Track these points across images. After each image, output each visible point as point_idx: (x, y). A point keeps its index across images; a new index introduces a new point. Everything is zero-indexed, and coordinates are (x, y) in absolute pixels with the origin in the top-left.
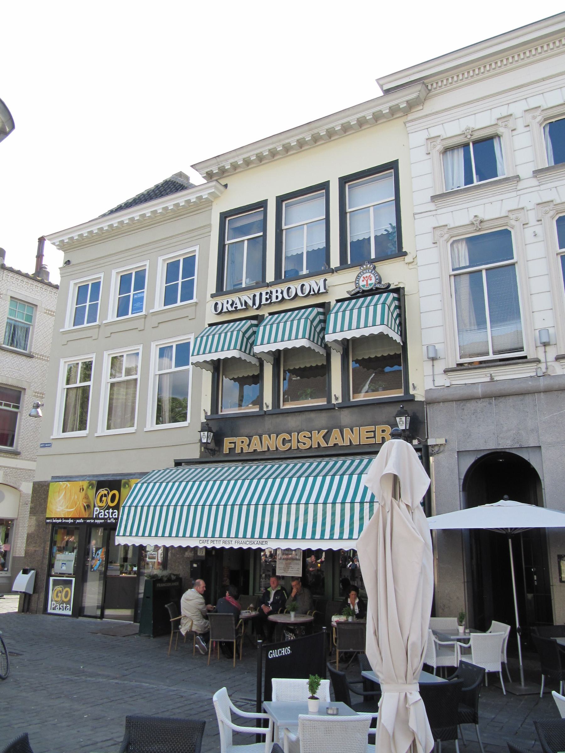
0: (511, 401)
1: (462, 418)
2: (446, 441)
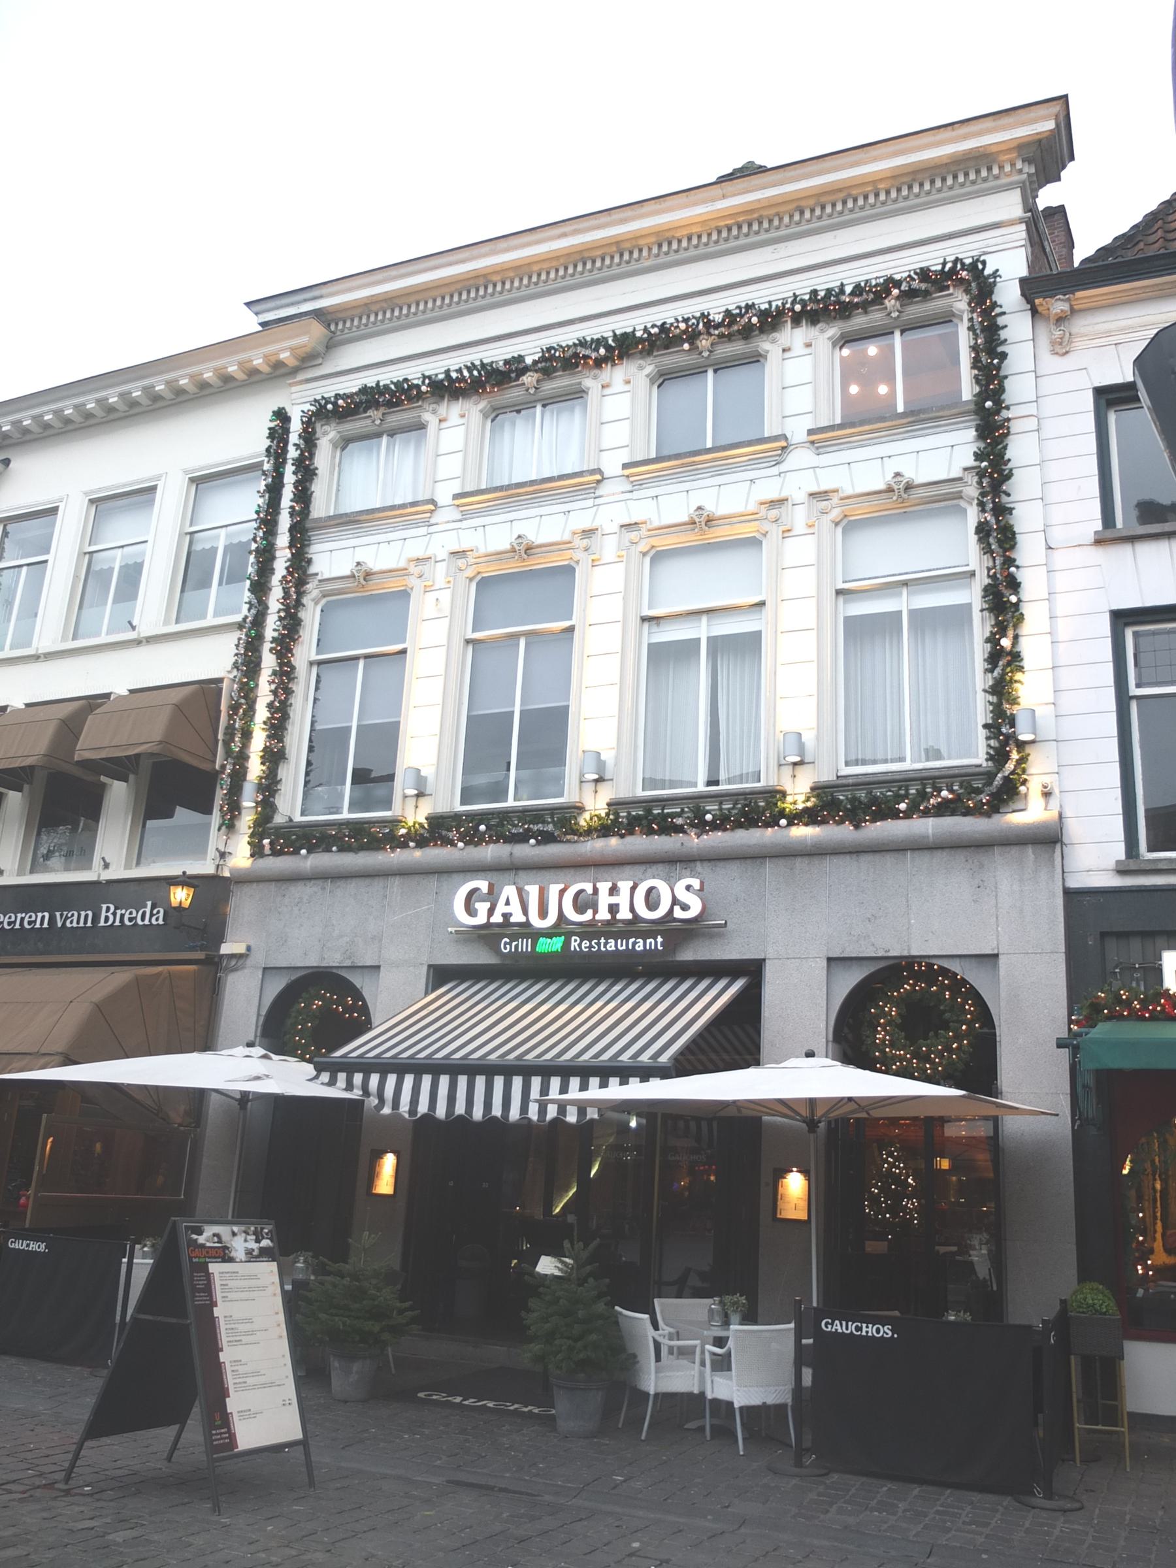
0: (352, 886)
1: (280, 910)
2: (249, 948)
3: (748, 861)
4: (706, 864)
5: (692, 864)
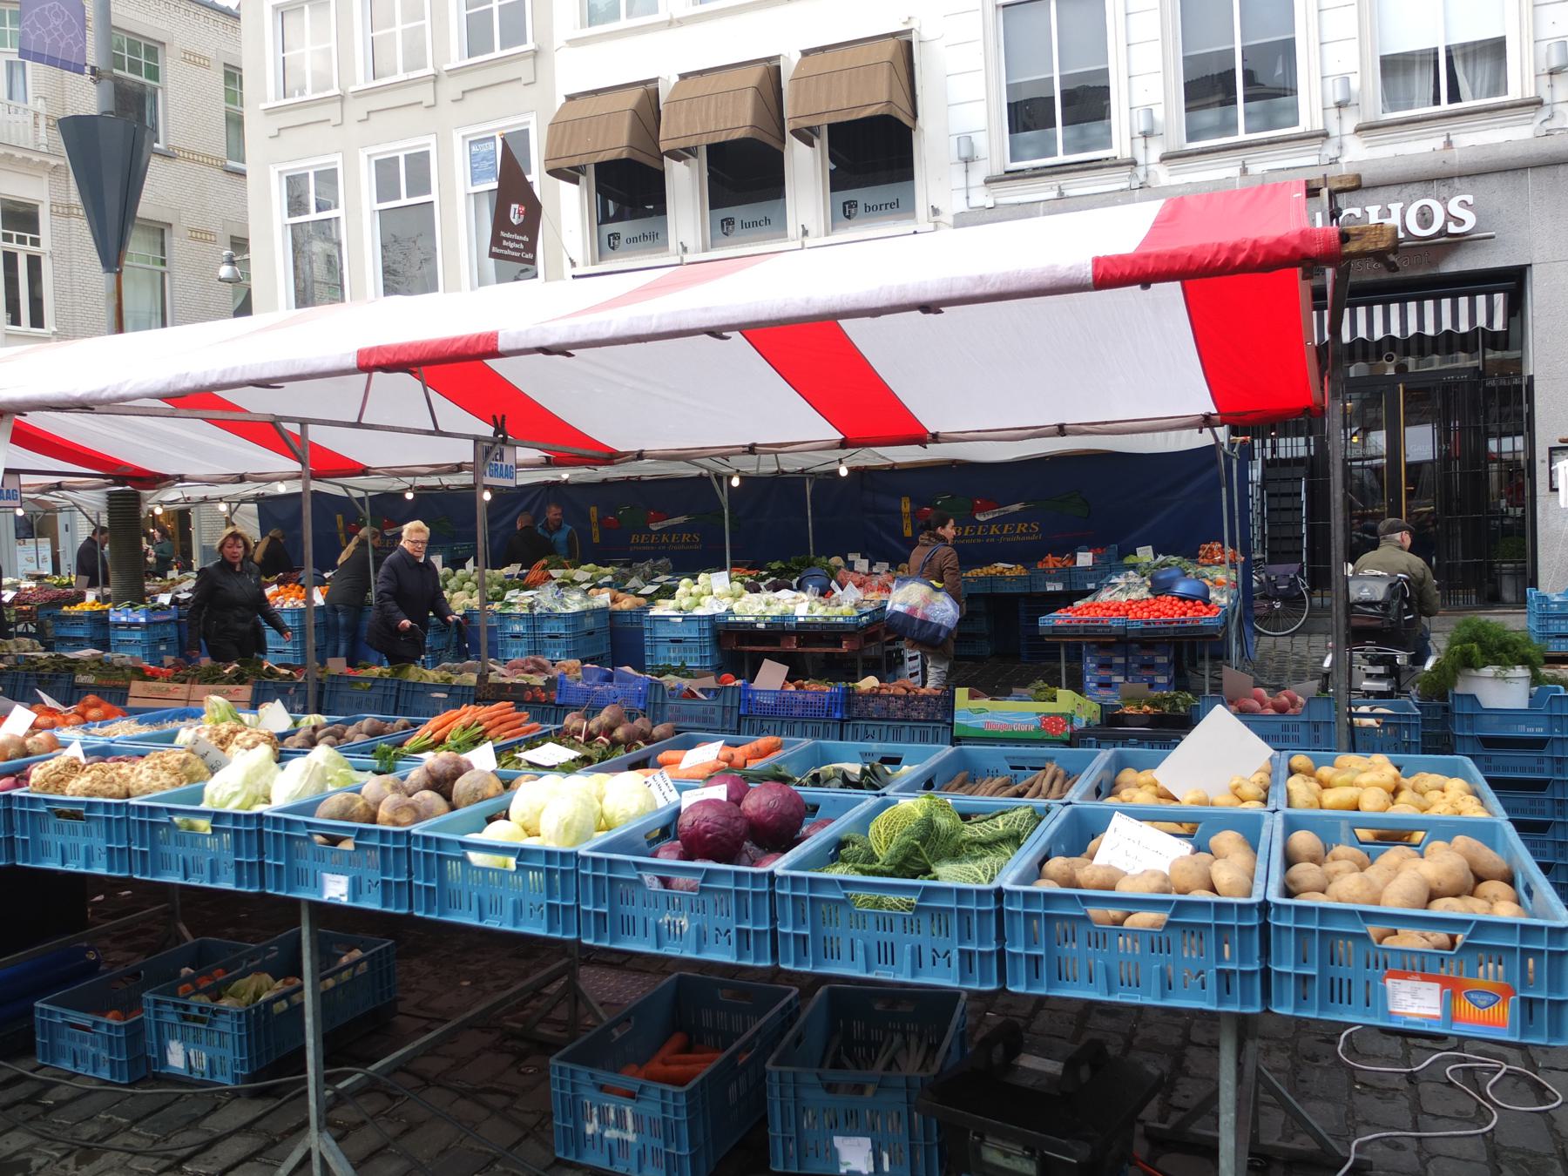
3: (1509, 173)
4: (1464, 180)
5: (1450, 181)
